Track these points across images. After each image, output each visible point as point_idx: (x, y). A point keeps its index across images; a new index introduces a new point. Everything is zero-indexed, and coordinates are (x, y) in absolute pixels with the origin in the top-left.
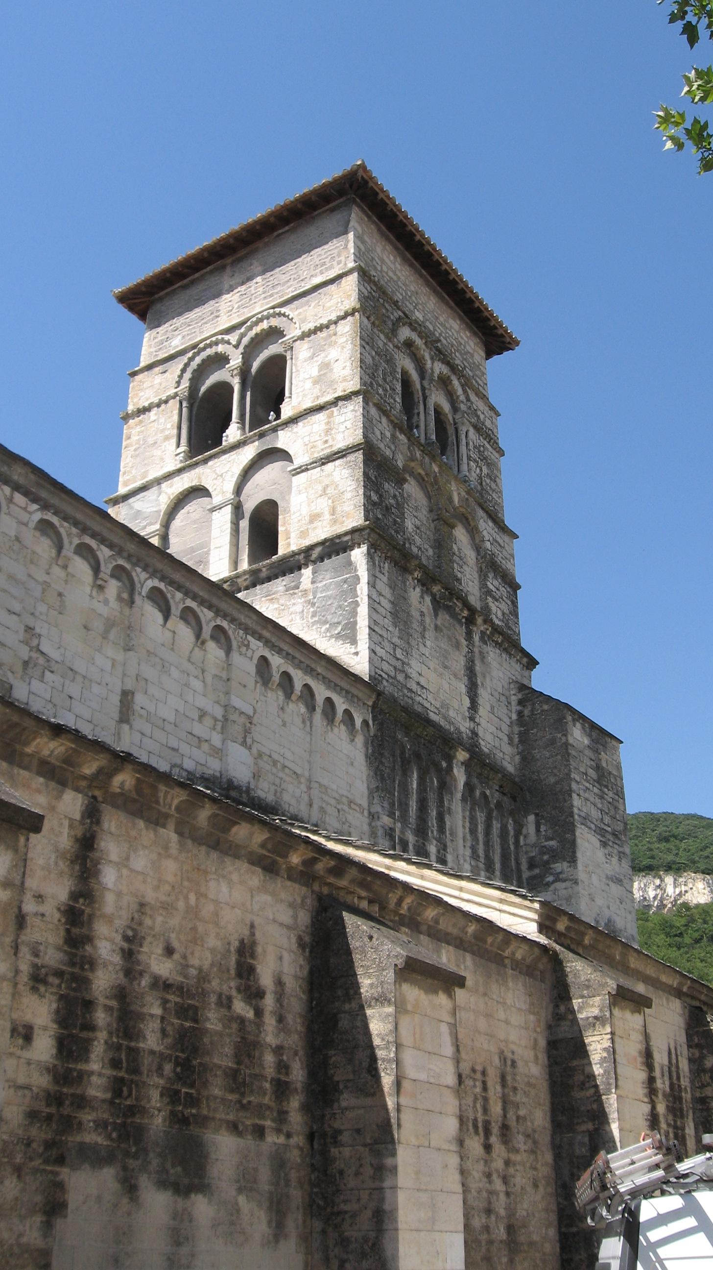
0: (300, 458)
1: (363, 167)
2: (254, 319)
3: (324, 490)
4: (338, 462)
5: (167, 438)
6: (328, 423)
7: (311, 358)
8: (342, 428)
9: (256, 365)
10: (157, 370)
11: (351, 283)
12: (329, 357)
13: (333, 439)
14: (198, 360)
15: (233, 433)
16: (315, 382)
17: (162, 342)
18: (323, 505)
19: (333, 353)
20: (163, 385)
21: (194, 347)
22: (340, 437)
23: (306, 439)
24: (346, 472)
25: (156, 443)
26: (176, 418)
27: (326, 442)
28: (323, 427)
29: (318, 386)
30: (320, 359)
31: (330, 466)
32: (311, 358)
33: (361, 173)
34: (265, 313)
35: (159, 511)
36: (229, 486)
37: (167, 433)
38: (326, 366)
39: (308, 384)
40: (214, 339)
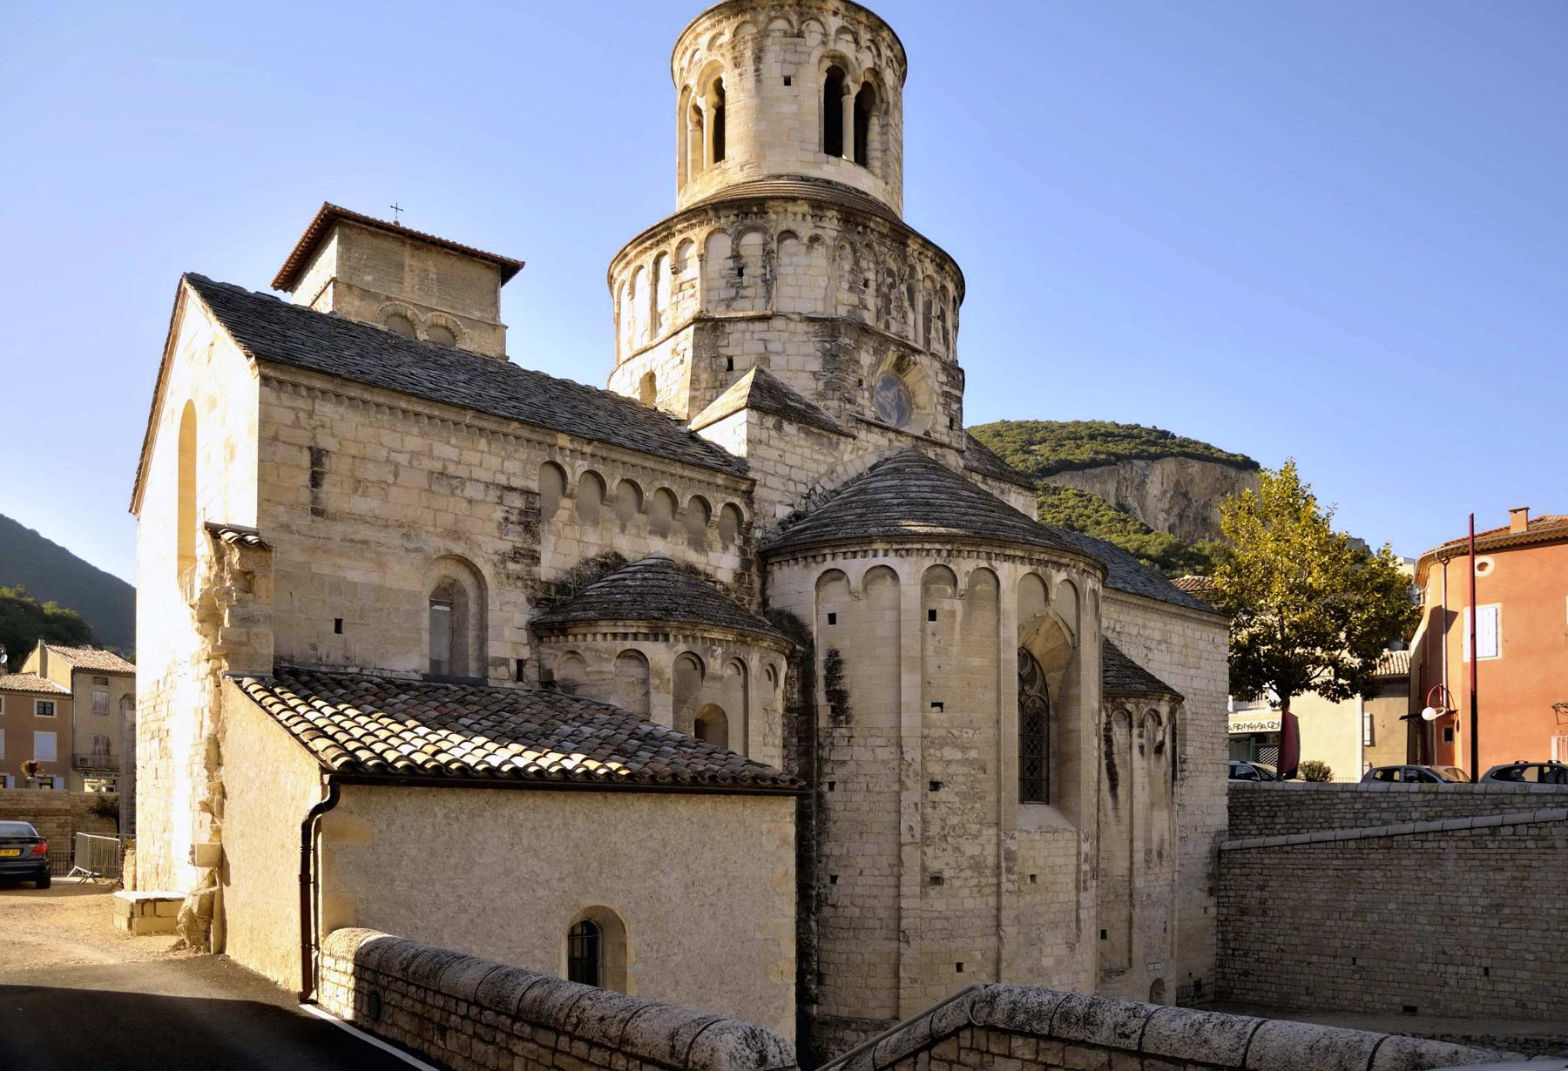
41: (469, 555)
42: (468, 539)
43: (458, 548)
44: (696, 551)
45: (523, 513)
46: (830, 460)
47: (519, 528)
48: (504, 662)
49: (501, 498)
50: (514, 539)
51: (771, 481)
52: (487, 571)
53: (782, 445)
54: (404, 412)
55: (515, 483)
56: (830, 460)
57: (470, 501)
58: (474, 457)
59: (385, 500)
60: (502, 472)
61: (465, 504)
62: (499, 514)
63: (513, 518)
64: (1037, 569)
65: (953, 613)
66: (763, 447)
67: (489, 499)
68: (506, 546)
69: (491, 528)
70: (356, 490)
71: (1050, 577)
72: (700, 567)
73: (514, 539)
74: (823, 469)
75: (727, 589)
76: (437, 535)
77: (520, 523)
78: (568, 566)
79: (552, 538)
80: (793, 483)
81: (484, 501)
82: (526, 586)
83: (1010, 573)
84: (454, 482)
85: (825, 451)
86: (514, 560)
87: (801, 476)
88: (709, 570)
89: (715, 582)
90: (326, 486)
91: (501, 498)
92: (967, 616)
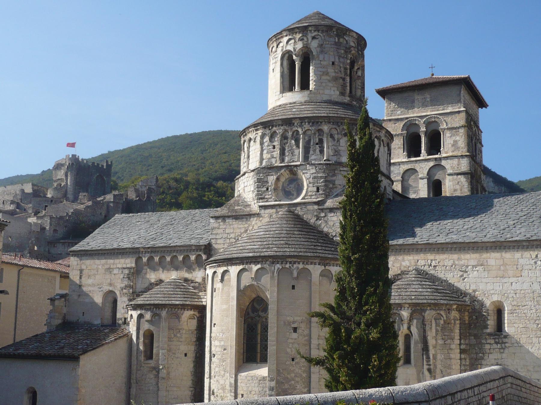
0: (450, 171)
1: (469, 77)
2: (430, 116)
3: (458, 182)
4: (462, 176)
5: (399, 148)
6: (458, 162)
7: (451, 137)
8: (463, 165)
9: (429, 131)
10: (392, 122)
11: (463, 115)
12: (457, 139)
13: (461, 168)
14: (408, 123)
15: (424, 154)
16: (452, 146)
17: (393, 111)
18: (458, 187)
19: (458, 138)
20: (396, 128)
21: (407, 118)
22: (463, 168)
23: (451, 165)
24: (465, 180)
25: (395, 148)
26: (402, 142)
27: (458, 168)
28: (457, 163)
29: (453, 147)
30: (454, 138)
31: (459, 176)
32: (451, 137)
33: (468, 79)
34: (434, 116)
35: (400, 173)
36: (426, 172)
37: (400, 146)
38: (456, 142)
39: (450, 146)
40: (415, 118)
41: (113, 290)
42: (114, 285)
43: (111, 289)
44: (188, 273)
45: (128, 274)
46: (246, 226)
47: (127, 279)
48: (121, 319)
49: (122, 271)
50: (126, 282)
51: (219, 241)
52: (118, 293)
53: (224, 227)
54: (102, 254)
55: (128, 266)
56: (246, 226)
57: (115, 274)
58: (117, 261)
59: (95, 279)
60: (125, 263)
61: (113, 276)
62: (122, 276)
63: (125, 277)
64: (245, 266)
65: (219, 288)
66: (217, 230)
67: (120, 272)
68: (123, 285)
69: (119, 281)
70: (88, 278)
71: (251, 268)
72: (190, 278)
73: (126, 282)
74: (243, 230)
75: (200, 284)
76: (106, 286)
77: (127, 278)
78: (145, 287)
79: (141, 279)
80: (228, 240)
81: (118, 274)
82: (128, 296)
83: (234, 270)
84: (111, 270)
85: (244, 223)
86: (125, 289)
87: (232, 236)
88: (193, 279)
89: (195, 283)
90: (83, 279)
91: (122, 271)
92: (223, 289)
